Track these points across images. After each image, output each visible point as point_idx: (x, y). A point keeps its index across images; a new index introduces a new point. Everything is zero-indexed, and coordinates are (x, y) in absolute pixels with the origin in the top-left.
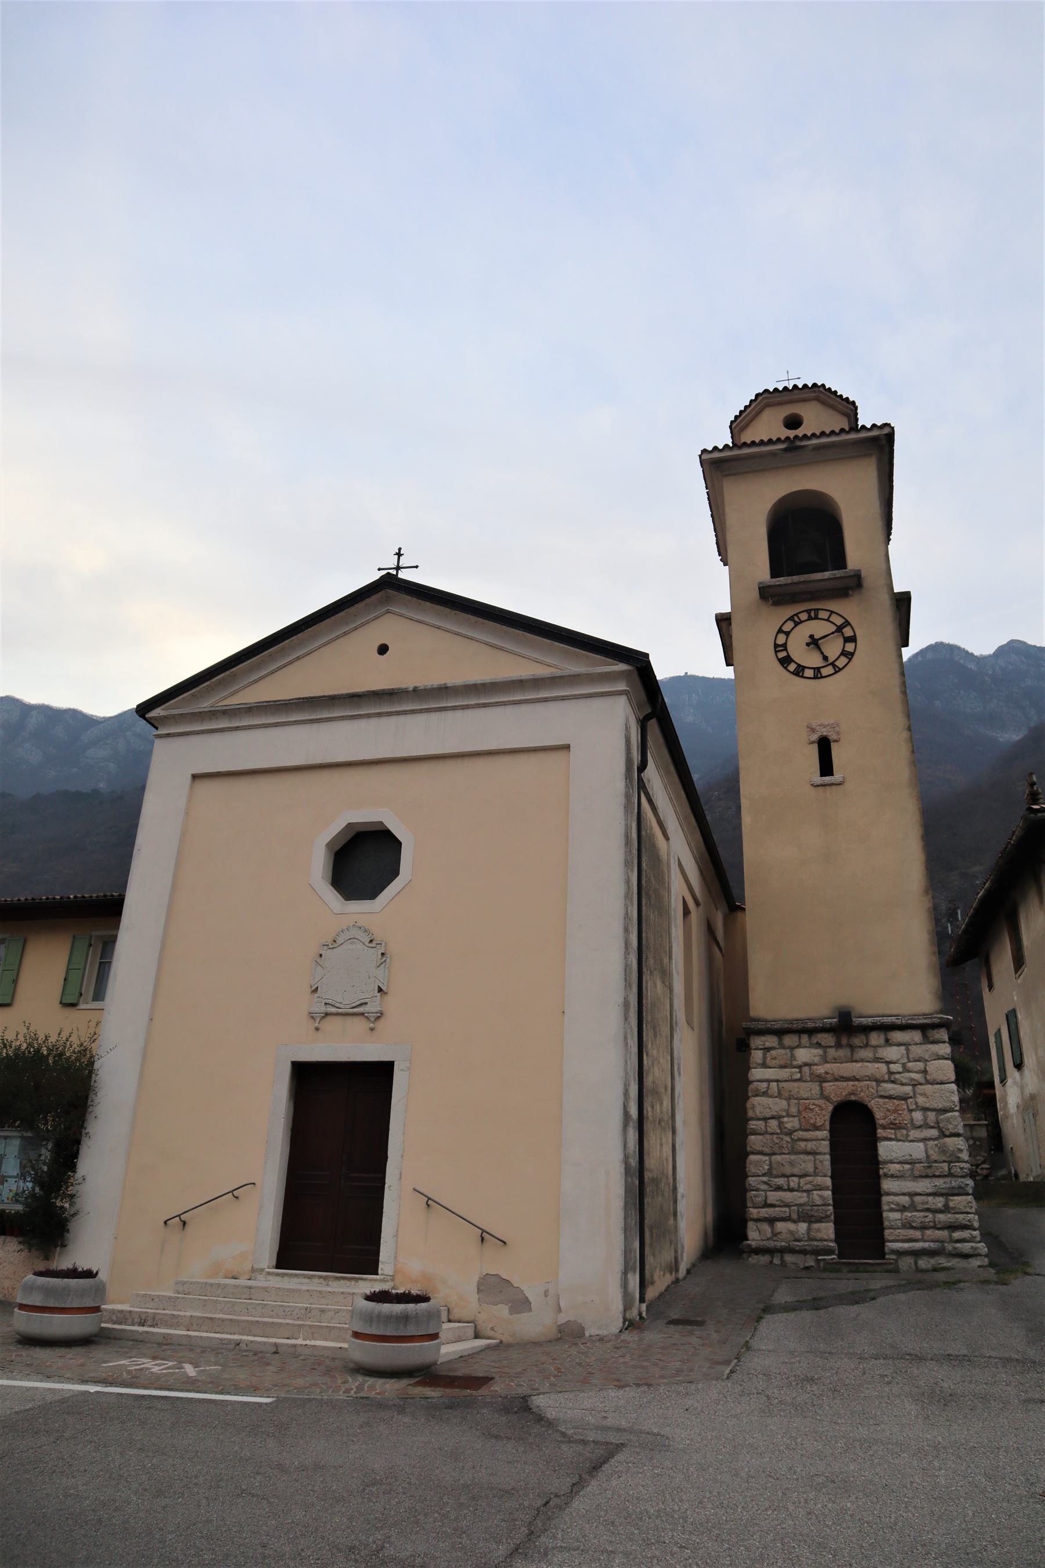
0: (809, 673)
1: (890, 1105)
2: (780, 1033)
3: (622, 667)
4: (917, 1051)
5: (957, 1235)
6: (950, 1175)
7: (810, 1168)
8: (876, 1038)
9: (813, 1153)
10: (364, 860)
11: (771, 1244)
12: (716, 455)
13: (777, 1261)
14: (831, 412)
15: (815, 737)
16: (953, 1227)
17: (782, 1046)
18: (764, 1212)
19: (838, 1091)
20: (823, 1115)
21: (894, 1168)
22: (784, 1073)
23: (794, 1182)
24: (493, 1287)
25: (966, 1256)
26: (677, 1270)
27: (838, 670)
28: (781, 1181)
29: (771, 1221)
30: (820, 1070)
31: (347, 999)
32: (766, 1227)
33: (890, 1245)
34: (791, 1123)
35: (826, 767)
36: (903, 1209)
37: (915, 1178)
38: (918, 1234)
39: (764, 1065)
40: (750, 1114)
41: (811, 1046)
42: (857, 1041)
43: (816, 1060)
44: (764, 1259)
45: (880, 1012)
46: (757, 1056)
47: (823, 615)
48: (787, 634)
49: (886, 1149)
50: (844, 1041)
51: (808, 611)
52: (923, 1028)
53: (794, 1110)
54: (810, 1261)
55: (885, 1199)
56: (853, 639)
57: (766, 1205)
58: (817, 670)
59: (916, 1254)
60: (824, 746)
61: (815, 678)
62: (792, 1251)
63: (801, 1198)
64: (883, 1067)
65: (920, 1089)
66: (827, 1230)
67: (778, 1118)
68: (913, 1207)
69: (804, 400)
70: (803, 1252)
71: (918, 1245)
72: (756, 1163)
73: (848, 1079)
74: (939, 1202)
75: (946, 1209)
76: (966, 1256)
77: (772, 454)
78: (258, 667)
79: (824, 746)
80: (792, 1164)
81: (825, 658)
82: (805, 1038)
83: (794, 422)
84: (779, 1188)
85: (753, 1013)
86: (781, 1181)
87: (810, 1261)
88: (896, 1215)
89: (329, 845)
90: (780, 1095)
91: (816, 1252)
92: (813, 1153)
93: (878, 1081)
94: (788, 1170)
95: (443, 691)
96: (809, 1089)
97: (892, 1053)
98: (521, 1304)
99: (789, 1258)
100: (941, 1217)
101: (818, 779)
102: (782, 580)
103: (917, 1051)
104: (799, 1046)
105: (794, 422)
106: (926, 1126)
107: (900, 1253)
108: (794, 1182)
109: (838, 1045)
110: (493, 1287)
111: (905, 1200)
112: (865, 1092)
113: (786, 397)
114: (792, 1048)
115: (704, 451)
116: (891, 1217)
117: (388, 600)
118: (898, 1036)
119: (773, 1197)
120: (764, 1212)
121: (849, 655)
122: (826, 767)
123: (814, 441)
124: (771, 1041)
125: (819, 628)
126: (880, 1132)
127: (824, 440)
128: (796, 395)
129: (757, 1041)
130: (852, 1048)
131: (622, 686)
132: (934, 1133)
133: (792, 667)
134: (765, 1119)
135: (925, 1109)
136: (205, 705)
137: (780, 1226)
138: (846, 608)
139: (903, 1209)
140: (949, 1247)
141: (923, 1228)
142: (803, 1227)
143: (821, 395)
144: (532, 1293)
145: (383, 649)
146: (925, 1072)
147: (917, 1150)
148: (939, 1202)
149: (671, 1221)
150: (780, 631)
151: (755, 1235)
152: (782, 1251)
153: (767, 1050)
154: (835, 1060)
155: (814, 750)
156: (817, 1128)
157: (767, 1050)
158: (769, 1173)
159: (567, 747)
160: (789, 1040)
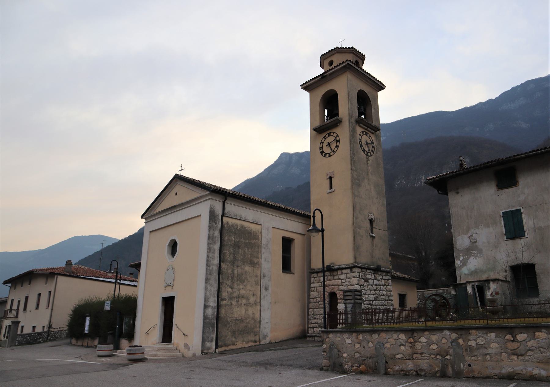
0: (327, 155)
3: (208, 192)
8: (339, 272)
10: (173, 247)
12: (304, 86)
14: (344, 54)
15: (328, 177)
24: (186, 345)
26: (260, 342)
27: (335, 153)
28: (315, 316)
29: (313, 328)
31: (168, 282)
32: (312, 330)
42: (335, 273)
44: (310, 339)
46: (312, 279)
47: (332, 134)
48: (323, 143)
52: (351, 268)
56: (338, 141)
58: (329, 154)
60: (331, 178)
64: (340, 281)
67: (316, 298)
69: (334, 54)
73: (332, 285)
77: (319, 80)
78: (158, 203)
79: (331, 178)
80: (318, 312)
81: (331, 149)
83: (331, 63)
84: (315, 319)
86: (315, 316)
89: (169, 245)
93: (339, 286)
94: (317, 313)
95: (182, 204)
97: (343, 277)
98: (189, 349)
99: (316, 338)
105: (331, 63)
109: (331, 275)
110: (186, 345)
112: (335, 290)
113: (328, 55)
115: (301, 85)
117: (176, 181)
118: (344, 271)
119: (314, 321)
121: (337, 147)
123: (328, 73)
124: (315, 275)
125: (330, 139)
126: (338, 301)
127: (331, 72)
128: (331, 53)
129: (313, 275)
130: (334, 276)
131: (210, 197)
133: (324, 154)
136: (151, 214)
138: (338, 131)
143: (337, 51)
144: (190, 347)
145: (176, 194)
149: (258, 329)
150: (321, 142)
152: (315, 336)
153: (315, 278)
154: (330, 280)
155: (328, 181)
157: (315, 278)
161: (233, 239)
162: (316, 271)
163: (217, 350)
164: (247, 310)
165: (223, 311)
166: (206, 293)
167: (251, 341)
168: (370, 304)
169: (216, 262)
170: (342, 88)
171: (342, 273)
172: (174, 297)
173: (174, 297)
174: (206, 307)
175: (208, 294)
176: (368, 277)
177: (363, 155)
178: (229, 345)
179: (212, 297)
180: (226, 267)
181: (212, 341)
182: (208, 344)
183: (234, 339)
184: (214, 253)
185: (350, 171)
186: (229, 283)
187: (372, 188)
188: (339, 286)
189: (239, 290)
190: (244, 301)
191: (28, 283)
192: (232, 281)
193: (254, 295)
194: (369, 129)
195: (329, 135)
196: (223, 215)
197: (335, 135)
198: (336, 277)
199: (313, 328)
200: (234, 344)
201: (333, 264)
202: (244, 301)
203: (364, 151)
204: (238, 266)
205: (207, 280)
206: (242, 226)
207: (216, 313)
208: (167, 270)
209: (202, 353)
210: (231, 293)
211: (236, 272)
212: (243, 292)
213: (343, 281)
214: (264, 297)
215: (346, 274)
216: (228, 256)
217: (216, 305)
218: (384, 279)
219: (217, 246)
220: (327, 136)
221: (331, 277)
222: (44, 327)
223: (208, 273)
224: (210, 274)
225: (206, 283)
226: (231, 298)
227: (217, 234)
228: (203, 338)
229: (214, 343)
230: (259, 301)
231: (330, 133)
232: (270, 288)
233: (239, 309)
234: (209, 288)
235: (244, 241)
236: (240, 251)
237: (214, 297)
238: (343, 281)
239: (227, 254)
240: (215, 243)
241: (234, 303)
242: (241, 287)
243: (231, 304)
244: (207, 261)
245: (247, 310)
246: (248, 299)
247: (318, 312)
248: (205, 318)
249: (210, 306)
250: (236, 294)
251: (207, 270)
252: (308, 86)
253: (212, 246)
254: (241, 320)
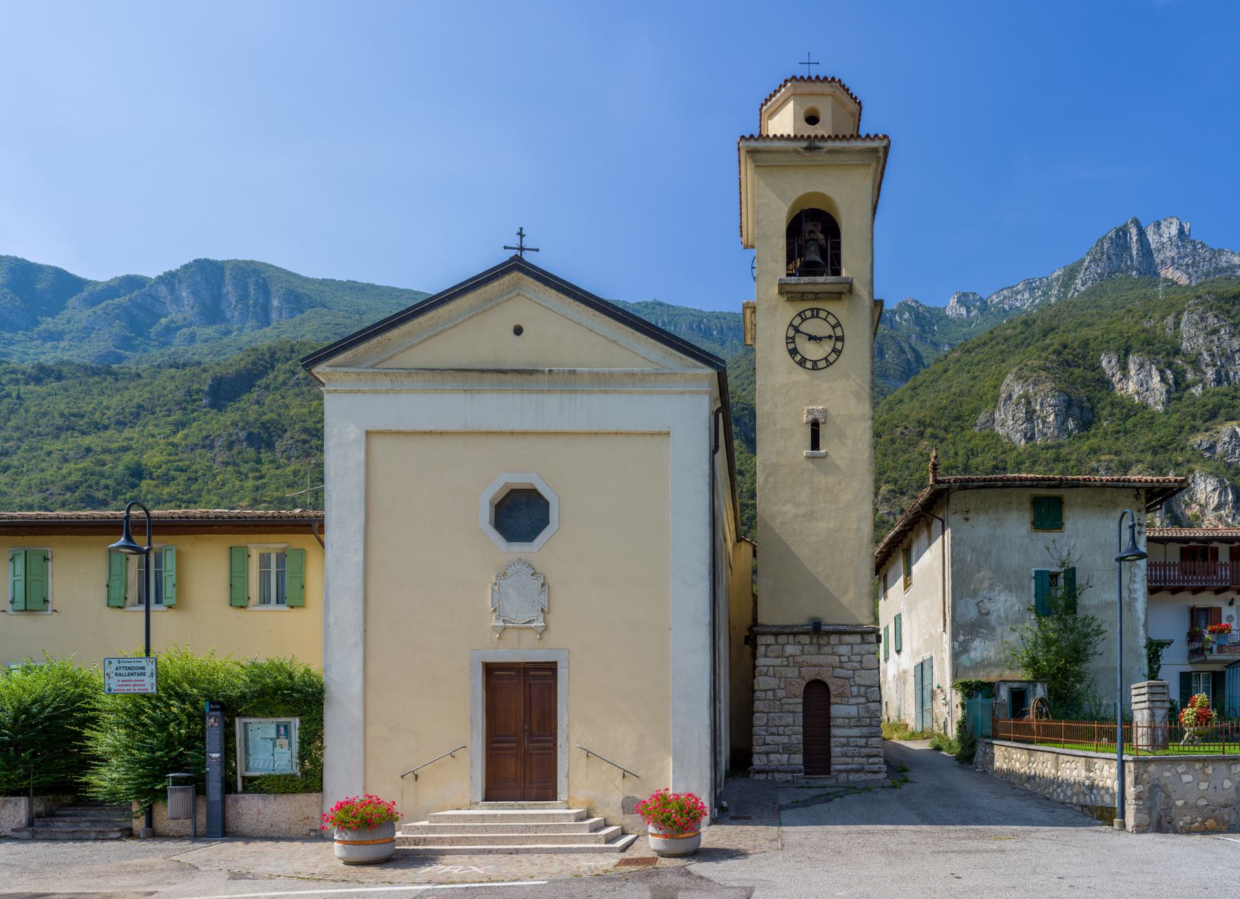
1: (840, 682)
2: (776, 634)
4: (857, 649)
5: (871, 760)
6: (870, 725)
7: (790, 721)
8: (834, 639)
9: (794, 712)
11: (767, 768)
13: (770, 778)
16: (869, 756)
17: (777, 643)
18: (763, 748)
19: (810, 674)
20: (799, 689)
21: (839, 721)
22: (777, 662)
23: (781, 730)
25: (875, 772)
28: (774, 730)
29: (767, 754)
30: (800, 659)
32: (763, 757)
33: (833, 767)
34: (781, 694)
35: (815, 445)
36: (843, 746)
37: (851, 727)
38: (850, 760)
39: (766, 656)
40: (756, 687)
41: (795, 644)
42: (823, 641)
43: (798, 653)
44: (762, 777)
45: (837, 622)
46: (761, 650)
47: (823, 314)
49: (837, 710)
50: (815, 641)
51: (812, 310)
53: (783, 685)
54: (789, 777)
55: (833, 740)
57: (764, 744)
58: (815, 362)
59: (848, 771)
61: (813, 369)
62: (779, 771)
63: (785, 740)
64: (837, 659)
65: (857, 673)
66: (798, 759)
67: (773, 690)
68: (848, 745)
70: (785, 772)
71: (850, 767)
72: (759, 720)
74: (862, 742)
75: (866, 745)
76: (875, 772)
79: (815, 426)
82: (791, 637)
84: (772, 734)
85: (760, 621)
87: (789, 777)
88: (839, 749)
90: (774, 676)
91: (793, 772)
93: (834, 668)
94: (778, 722)
96: (792, 673)
97: (843, 650)
99: (777, 775)
100: (863, 750)
101: (807, 451)
102: (793, 279)
103: (857, 649)
104: (788, 643)
106: (859, 695)
107: (840, 771)
108: (781, 730)
109: (811, 643)
111: (844, 740)
112: (825, 676)
114: (783, 645)
116: (836, 751)
118: (847, 638)
120: (763, 748)
122: (815, 445)
124: (770, 639)
126: (833, 700)
132: (863, 700)
134: (765, 691)
135: (860, 685)
137: (772, 756)
139: (843, 746)
140: (866, 767)
141: (853, 756)
142: (786, 757)
146: (861, 662)
147: (853, 711)
148: (862, 742)
151: (758, 761)
152: (772, 771)
153: (768, 645)
155: (808, 430)
156: (796, 697)
158: (766, 725)
160: (782, 639)
162: (775, 630)
195: (815, 314)
198: (827, 650)
199: (767, 754)
215: (852, 645)
220: (809, 314)
221: (813, 649)
238: (844, 659)
247: (780, 718)
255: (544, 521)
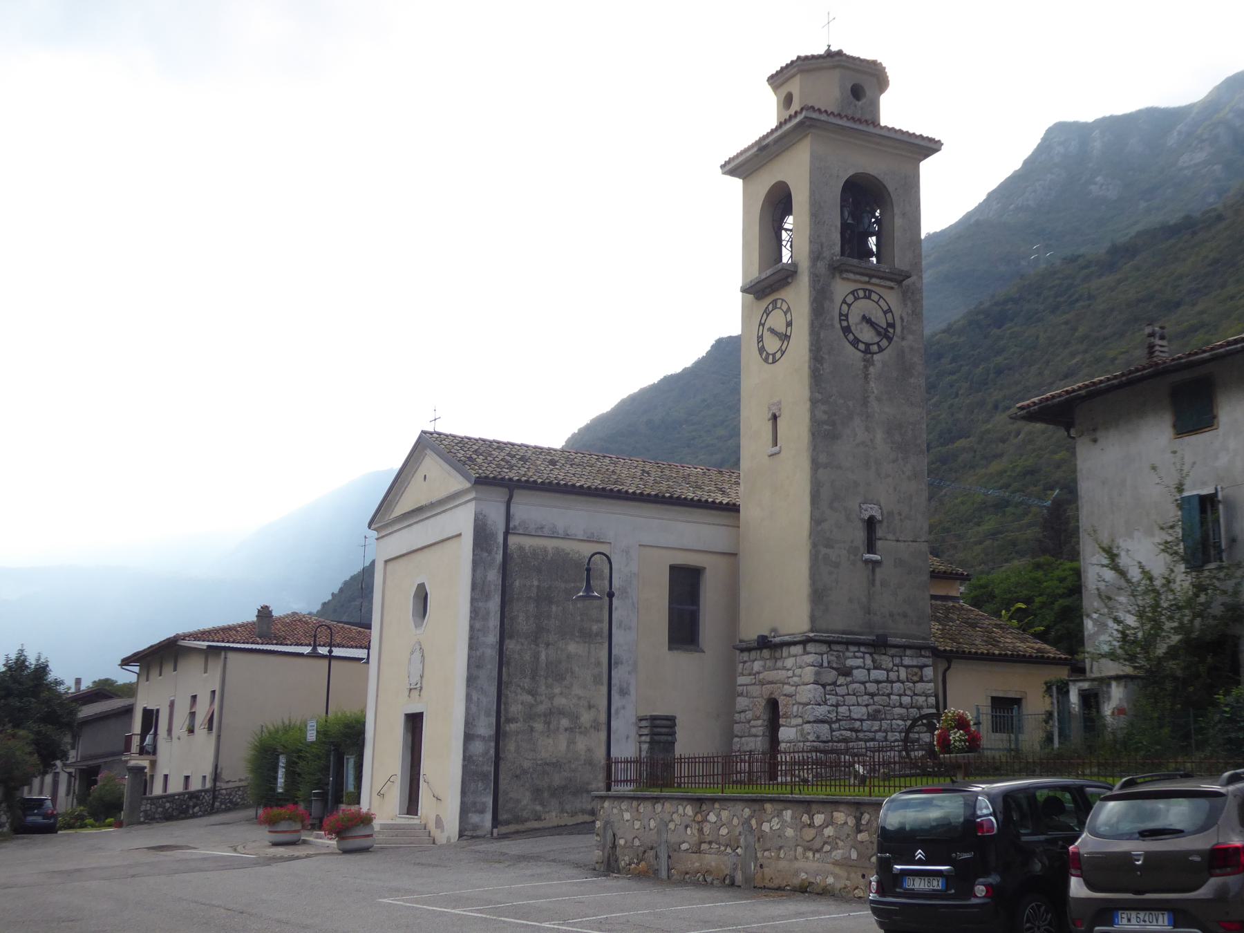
9: (756, 736)
52: (805, 642)
60: (775, 418)
79: (775, 418)
92: (756, 736)
115: (722, 167)
126: (781, 721)
130: (776, 659)
131: (473, 495)
132: (800, 721)
153: (745, 662)
155: (770, 425)
157: (745, 662)
159: (460, 535)
161: (536, 583)
163: (495, 831)
164: (571, 742)
165: (510, 746)
166: (468, 709)
167: (583, 812)
168: (851, 730)
169: (492, 638)
170: (833, 153)
171: (790, 656)
172: (422, 714)
173: (422, 714)
174: (468, 737)
175: (474, 709)
176: (850, 663)
177: (853, 355)
178: (527, 820)
179: (482, 717)
180: (518, 647)
181: (482, 812)
182: (474, 818)
183: (538, 808)
184: (486, 618)
185: (808, 405)
186: (527, 683)
187: (879, 436)
188: (784, 684)
189: (551, 698)
190: (565, 722)
191: (172, 668)
192: (533, 678)
193: (590, 707)
194: (874, 280)
196: (506, 533)
197: (785, 307)
200: (539, 819)
201: (774, 630)
202: (565, 722)
203: (855, 342)
204: (548, 645)
205: (471, 680)
206: (558, 551)
207: (492, 752)
208: (412, 653)
209: (461, 836)
210: (531, 706)
211: (543, 657)
212: (560, 701)
213: (790, 673)
214: (617, 712)
216: (523, 623)
217: (492, 732)
218: (907, 667)
219: (494, 604)
222: (204, 777)
223: (474, 664)
224: (478, 667)
225: (468, 686)
226: (530, 717)
227: (494, 576)
228: (463, 803)
229: (488, 817)
230: (603, 717)
231: (775, 301)
232: (633, 691)
233: (550, 741)
234: (475, 698)
235: (563, 585)
236: (554, 608)
237: (488, 715)
239: (521, 618)
240: (488, 597)
241: (539, 726)
242: (557, 691)
243: (532, 729)
244: (471, 638)
245: (571, 742)
246: (575, 717)
248: (467, 759)
249: (479, 736)
250: (542, 708)
251: (470, 657)
252: (741, 167)
253: (480, 604)
254: (557, 765)
255: (267, 607)
